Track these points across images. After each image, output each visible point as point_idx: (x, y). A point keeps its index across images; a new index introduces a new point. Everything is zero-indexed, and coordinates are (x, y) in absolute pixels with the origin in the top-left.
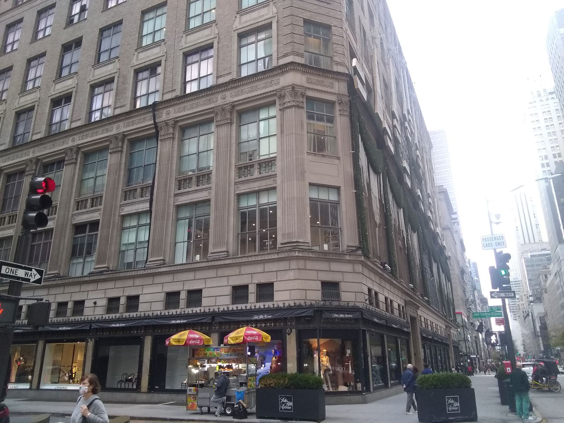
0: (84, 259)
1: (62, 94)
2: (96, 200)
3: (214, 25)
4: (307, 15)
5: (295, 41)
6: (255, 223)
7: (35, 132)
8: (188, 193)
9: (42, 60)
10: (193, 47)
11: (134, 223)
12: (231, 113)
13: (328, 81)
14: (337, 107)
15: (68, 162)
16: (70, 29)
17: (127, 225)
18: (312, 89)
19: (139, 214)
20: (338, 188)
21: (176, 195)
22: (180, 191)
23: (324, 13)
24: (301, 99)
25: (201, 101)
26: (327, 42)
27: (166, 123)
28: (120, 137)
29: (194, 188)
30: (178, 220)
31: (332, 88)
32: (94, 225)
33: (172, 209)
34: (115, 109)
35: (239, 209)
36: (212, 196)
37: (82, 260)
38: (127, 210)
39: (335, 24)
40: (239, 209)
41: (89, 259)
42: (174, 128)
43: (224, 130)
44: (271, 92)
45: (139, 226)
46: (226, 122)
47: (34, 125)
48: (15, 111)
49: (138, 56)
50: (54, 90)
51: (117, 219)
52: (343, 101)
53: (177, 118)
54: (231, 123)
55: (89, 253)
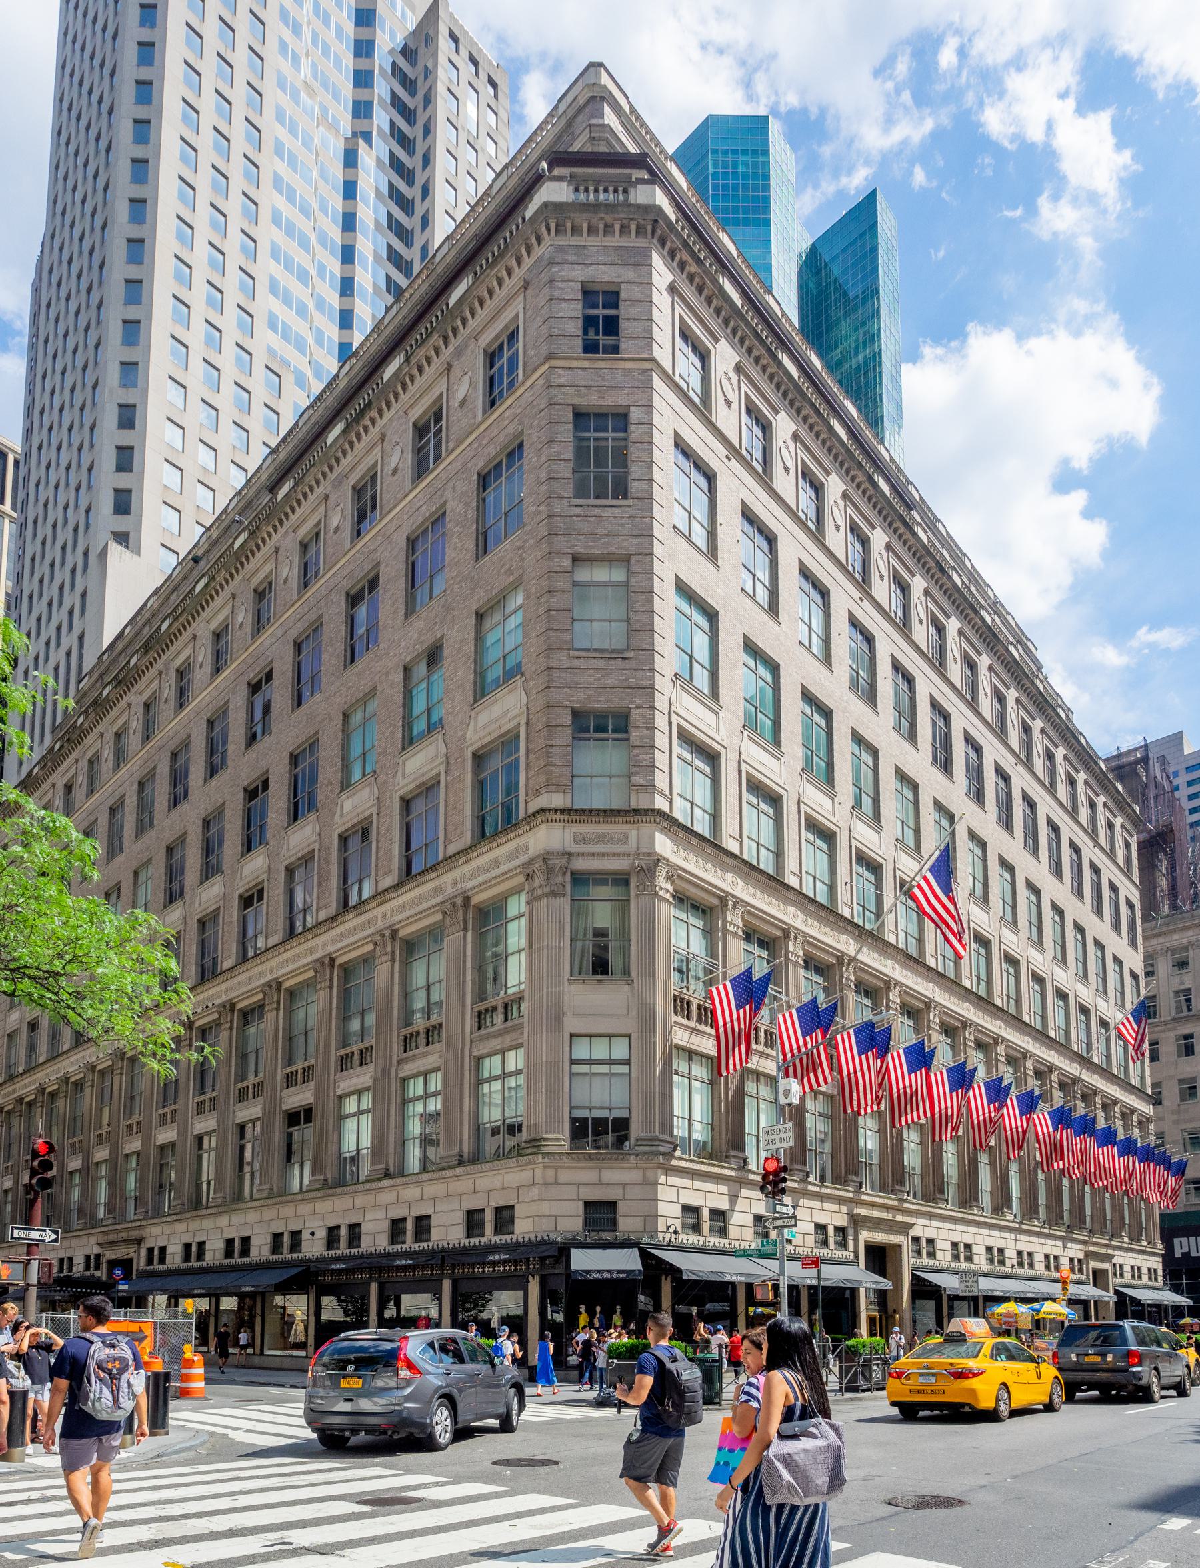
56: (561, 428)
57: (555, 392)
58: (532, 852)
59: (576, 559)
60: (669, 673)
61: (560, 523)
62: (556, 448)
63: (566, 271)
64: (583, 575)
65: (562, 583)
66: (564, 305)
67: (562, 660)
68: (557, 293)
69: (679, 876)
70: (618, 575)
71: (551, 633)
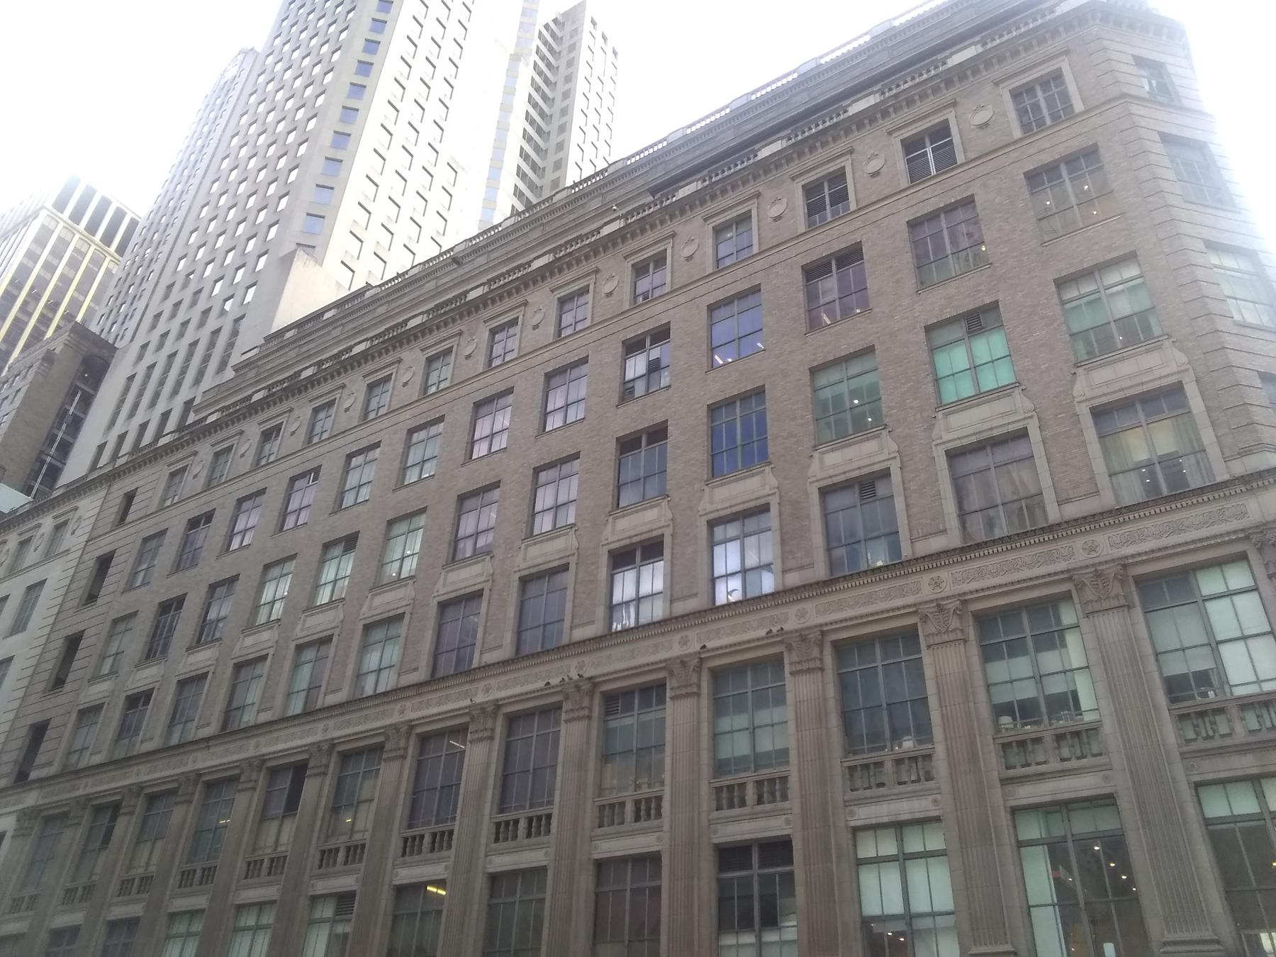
0: (759, 937)
1: (635, 540)
2: (772, 790)
3: (1017, 391)
7: (576, 621)
8: (1041, 777)
9: (566, 468)
11: (888, 847)
15: (678, 692)
16: (632, 408)
17: (867, 849)
21: (1005, 782)
22: (1012, 773)
25: (1027, 554)
27: (938, 605)
28: (814, 635)
29: (1055, 765)
32: (778, 850)
33: (1004, 819)
34: (784, 572)
36: (1120, 783)
37: (748, 939)
38: (865, 814)
40: (1207, 822)
41: (770, 937)
42: (961, 617)
43: (1111, 625)
44: (1228, 533)
46: (1114, 603)
47: (574, 607)
48: (518, 575)
49: (822, 461)
50: (613, 532)
51: (846, 837)
53: (965, 594)
55: (771, 920)
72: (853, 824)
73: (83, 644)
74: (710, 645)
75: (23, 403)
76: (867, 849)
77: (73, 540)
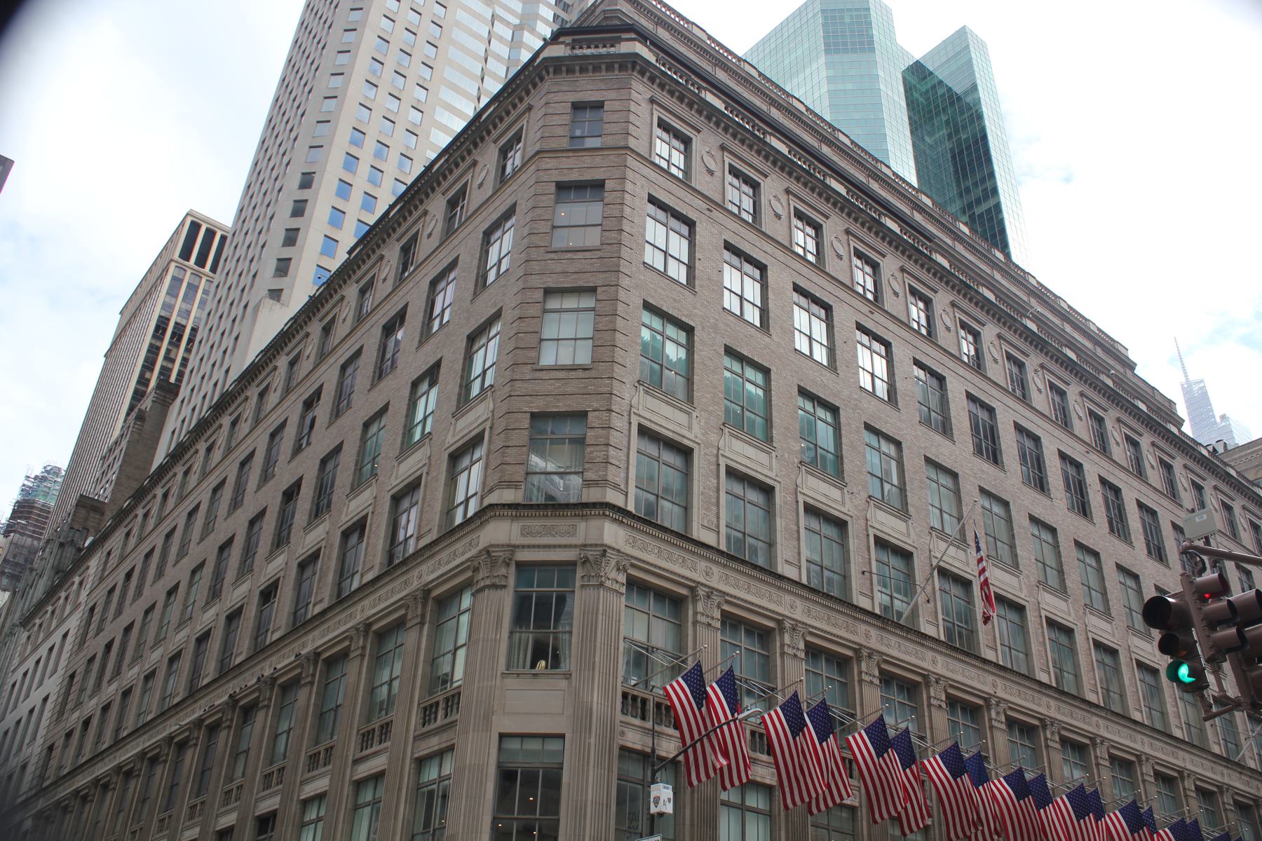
4: (538, 405)
5: (508, 460)
6: (535, 797)
10: (401, 486)
12: (424, 605)
13: (562, 524)
14: (580, 572)
18: (529, 546)
19: (320, 797)
20: (562, 736)
21: (357, 762)
23: (576, 390)
24: (503, 571)
26: (580, 442)
30: (356, 807)
31: (574, 535)
35: (418, 787)
38: (310, 790)
39: (596, 405)
45: (319, 819)
52: (591, 558)
54: (422, 624)
56: (543, 198)
57: (541, 173)
58: (481, 547)
59: (549, 292)
60: (630, 379)
61: (536, 267)
62: (538, 211)
63: (560, 97)
64: (553, 304)
65: (533, 310)
66: (555, 117)
67: (526, 372)
68: (550, 111)
69: (633, 566)
70: (587, 302)
71: (518, 351)
72: (302, 797)
73: (76, 679)
74: (279, 667)
75: (124, 460)
76: (312, 815)
77: (84, 594)
